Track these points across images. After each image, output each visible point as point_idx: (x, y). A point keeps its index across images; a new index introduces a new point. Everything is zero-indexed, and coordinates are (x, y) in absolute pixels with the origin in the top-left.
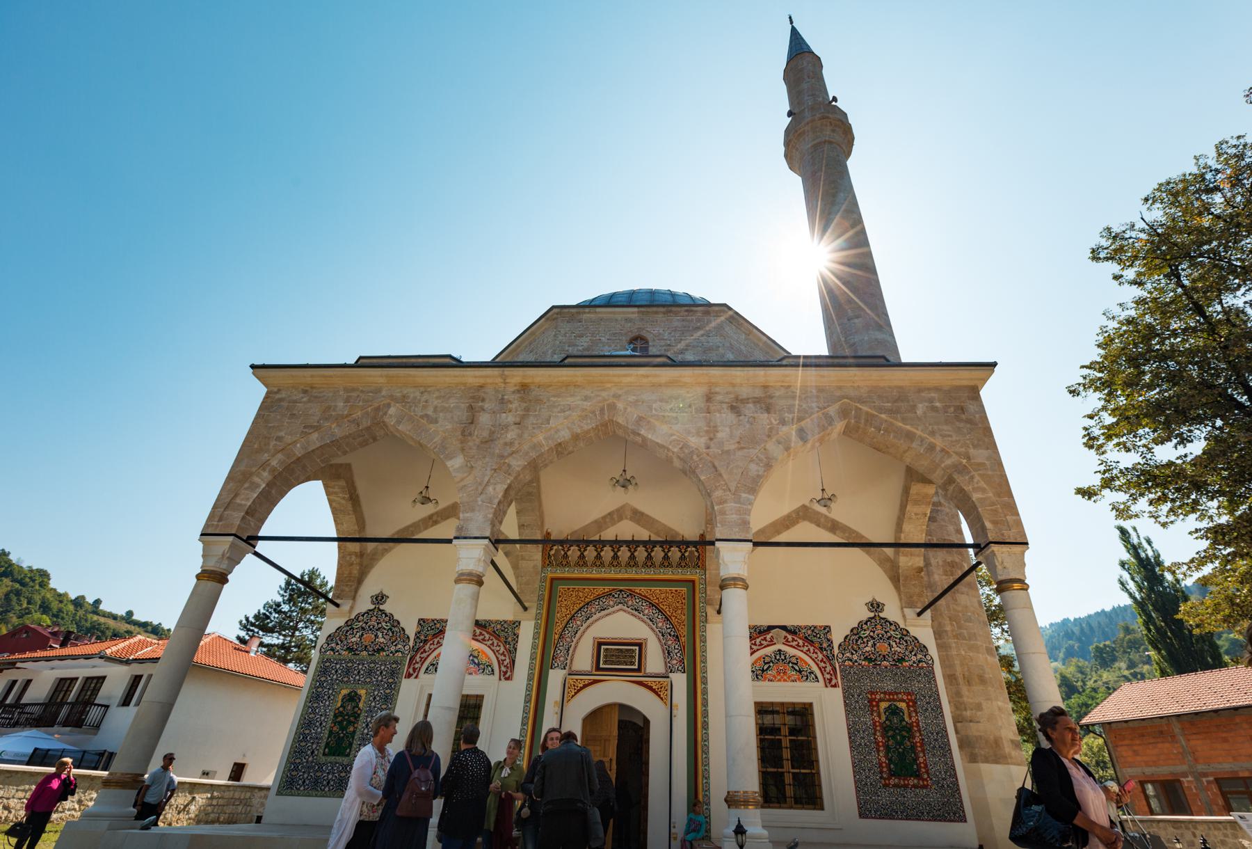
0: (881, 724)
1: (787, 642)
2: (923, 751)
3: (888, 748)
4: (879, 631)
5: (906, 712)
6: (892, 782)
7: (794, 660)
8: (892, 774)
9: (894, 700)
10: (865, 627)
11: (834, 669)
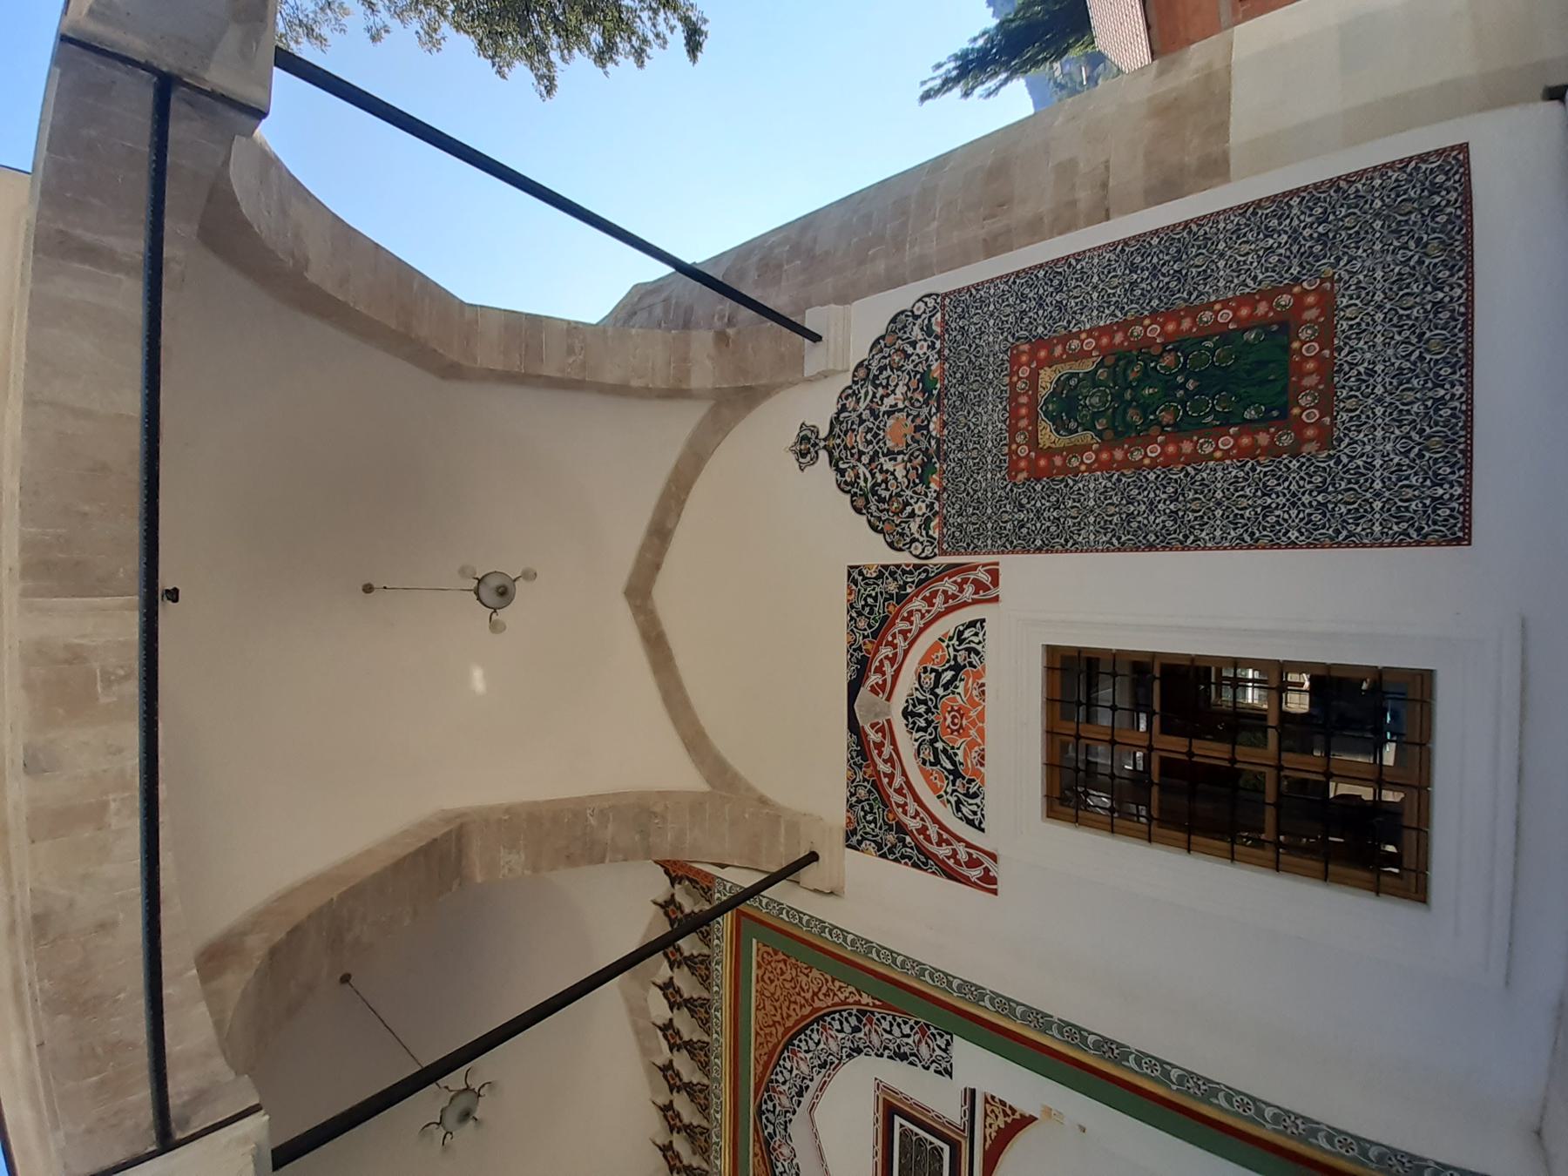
0: (1107, 445)
1: (885, 690)
2: (1193, 312)
3: (1179, 430)
4: (858, 439)
5: (1066, 369)
7: (929, 679)
8: (1280, 414)
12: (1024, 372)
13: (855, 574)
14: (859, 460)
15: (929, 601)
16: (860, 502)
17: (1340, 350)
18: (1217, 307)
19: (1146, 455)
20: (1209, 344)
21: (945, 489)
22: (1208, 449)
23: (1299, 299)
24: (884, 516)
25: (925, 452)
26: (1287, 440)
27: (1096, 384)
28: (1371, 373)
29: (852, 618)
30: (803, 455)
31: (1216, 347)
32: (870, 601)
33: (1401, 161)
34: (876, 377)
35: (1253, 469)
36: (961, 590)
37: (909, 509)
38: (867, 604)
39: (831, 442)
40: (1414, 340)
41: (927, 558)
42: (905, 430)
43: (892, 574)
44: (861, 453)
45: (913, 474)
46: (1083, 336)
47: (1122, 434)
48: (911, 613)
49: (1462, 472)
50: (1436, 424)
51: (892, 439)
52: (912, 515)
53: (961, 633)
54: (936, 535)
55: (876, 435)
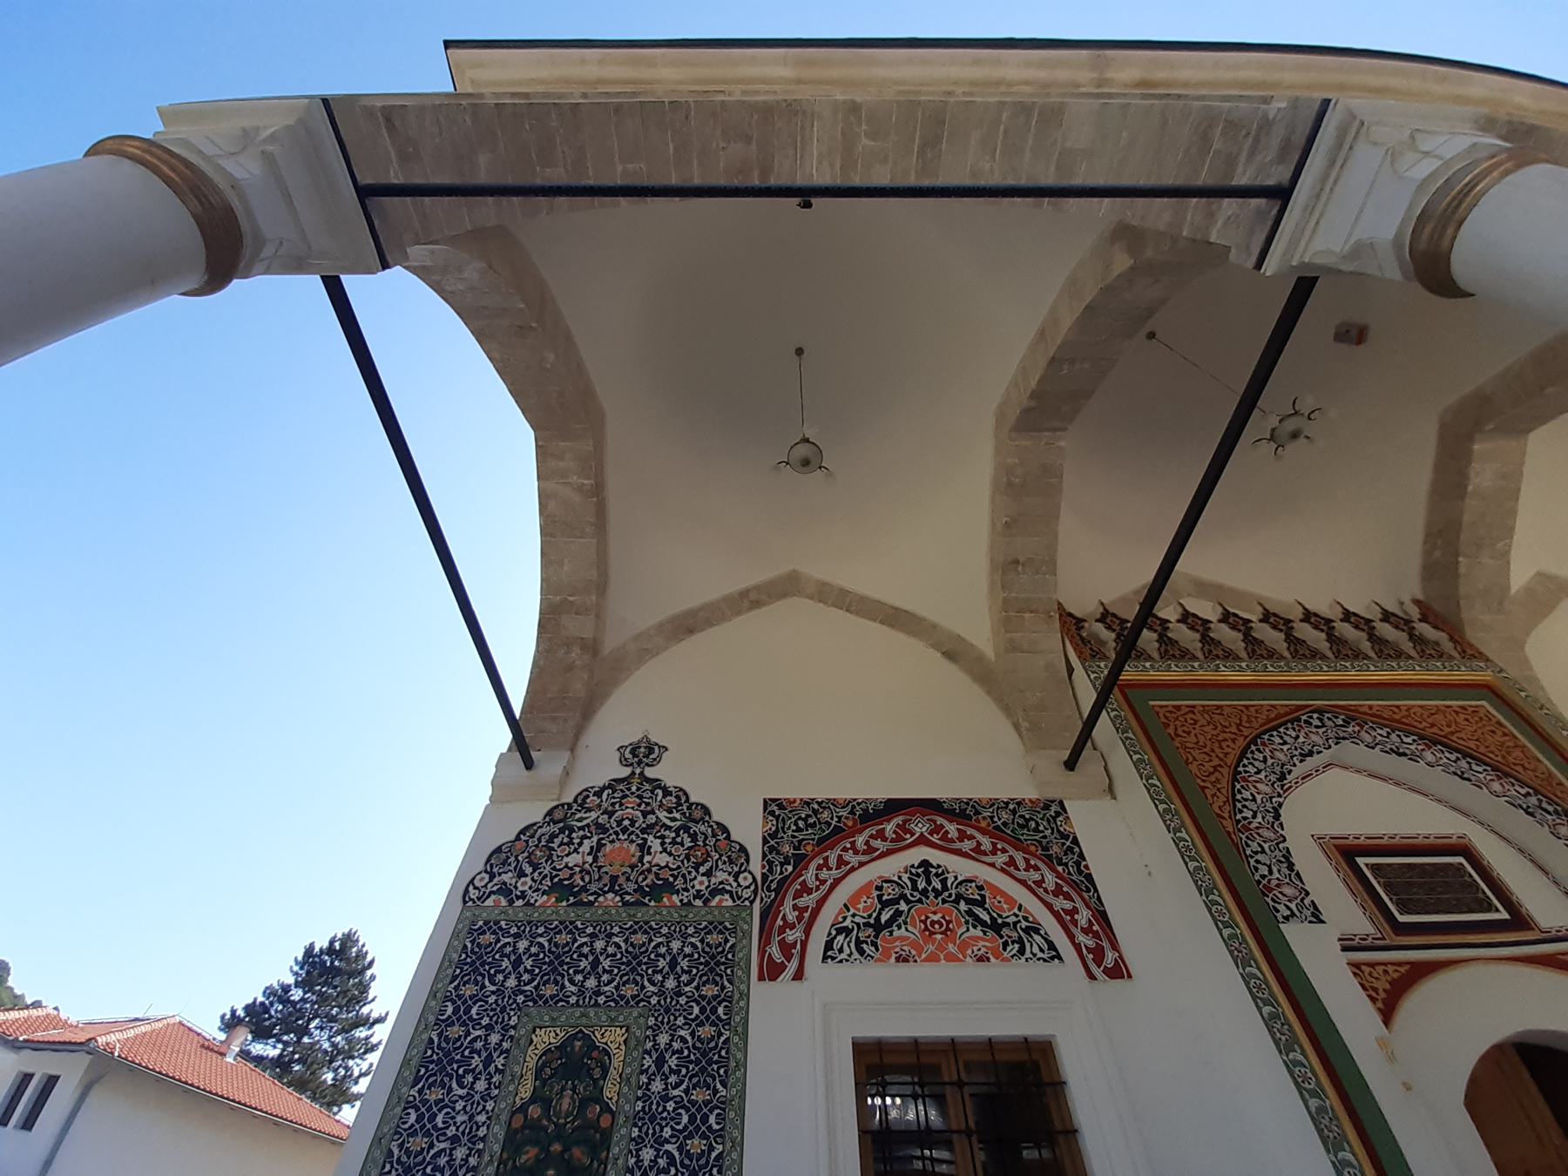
16: (558, 815)
25: (584, 889)
27: (584, 1104)
30: (634, 752)
34: (687, 829)
37: (528, 870)
39: (636, 780)
44: (611, 814)
52: (522, 874)
55: (624, 830)
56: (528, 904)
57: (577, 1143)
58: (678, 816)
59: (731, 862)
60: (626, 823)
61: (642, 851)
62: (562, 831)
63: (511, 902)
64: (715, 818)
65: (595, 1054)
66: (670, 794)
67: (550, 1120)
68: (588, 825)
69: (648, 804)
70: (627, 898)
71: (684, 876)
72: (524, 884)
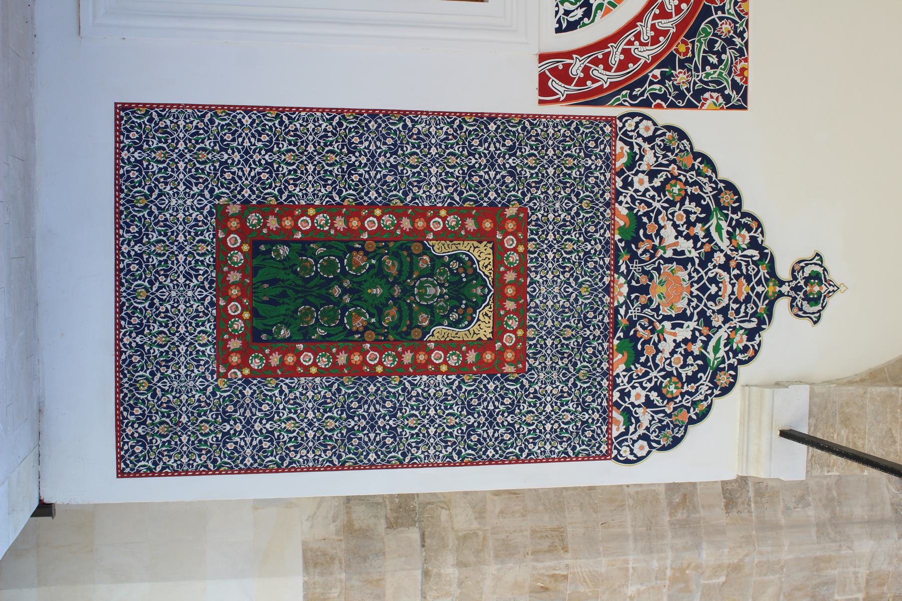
0: (419, 235)
2: (335, 370)
3: (345, 244)
4: (729, 288)
5: (461, 334)
6: (234, 240)
8: (260, 245)
9: (500, 298)
10: (742, 238)
11: (599, 98)
12: (509, 339)
13: (735, 97)
14: (728, 258)
15: (628, 57)
16: (727, 198)
17: (212, 303)
18: (314, 370)
19: (379, 219)
20: (321, 332)
21: (608, 204)
22: (321, 219)
23: (244, 363)
24: (692, 176)
25: (634, 256)
26: (253, 219)
27: (430, 309)
28: (188, 277)
29: (741, 35)
30: (815, 276)
31: (314, 327)
32: (713, 59)
33: (167, 475)
34: (703, 369)
35: (281, 192)
36: (586, 70)
37: (657, 183)
38: (718, 54)
39: (771, 289)
40: (156, 301)
41: (632, 115)
42: (662, 290)
43: (681, 95)
44: (725, 267)
45: (651, 229)
46: (444, 368)
47: (401, 247)
48: (655, 41)
49: (121, 172)
50: (140, 218)
51: (678, 281)
52: (652, 175)
53: (587, 14)
54: (619, 144)
55: (703, 289)
56: (618, 193)
57: (400, 310)
58: (721, 353)
59: (662, 429)
60: (713, 289)
61: (678, 317)
62: (706, 209)
63: (620, 173)
64: (718, 403)
65: (470, 310)
66: (751, 338)
67: (418, 278)
68: (712, 240)
69: (737, 312)
70: (622, 311)
71: (646, 374)
72: (641, 182)
